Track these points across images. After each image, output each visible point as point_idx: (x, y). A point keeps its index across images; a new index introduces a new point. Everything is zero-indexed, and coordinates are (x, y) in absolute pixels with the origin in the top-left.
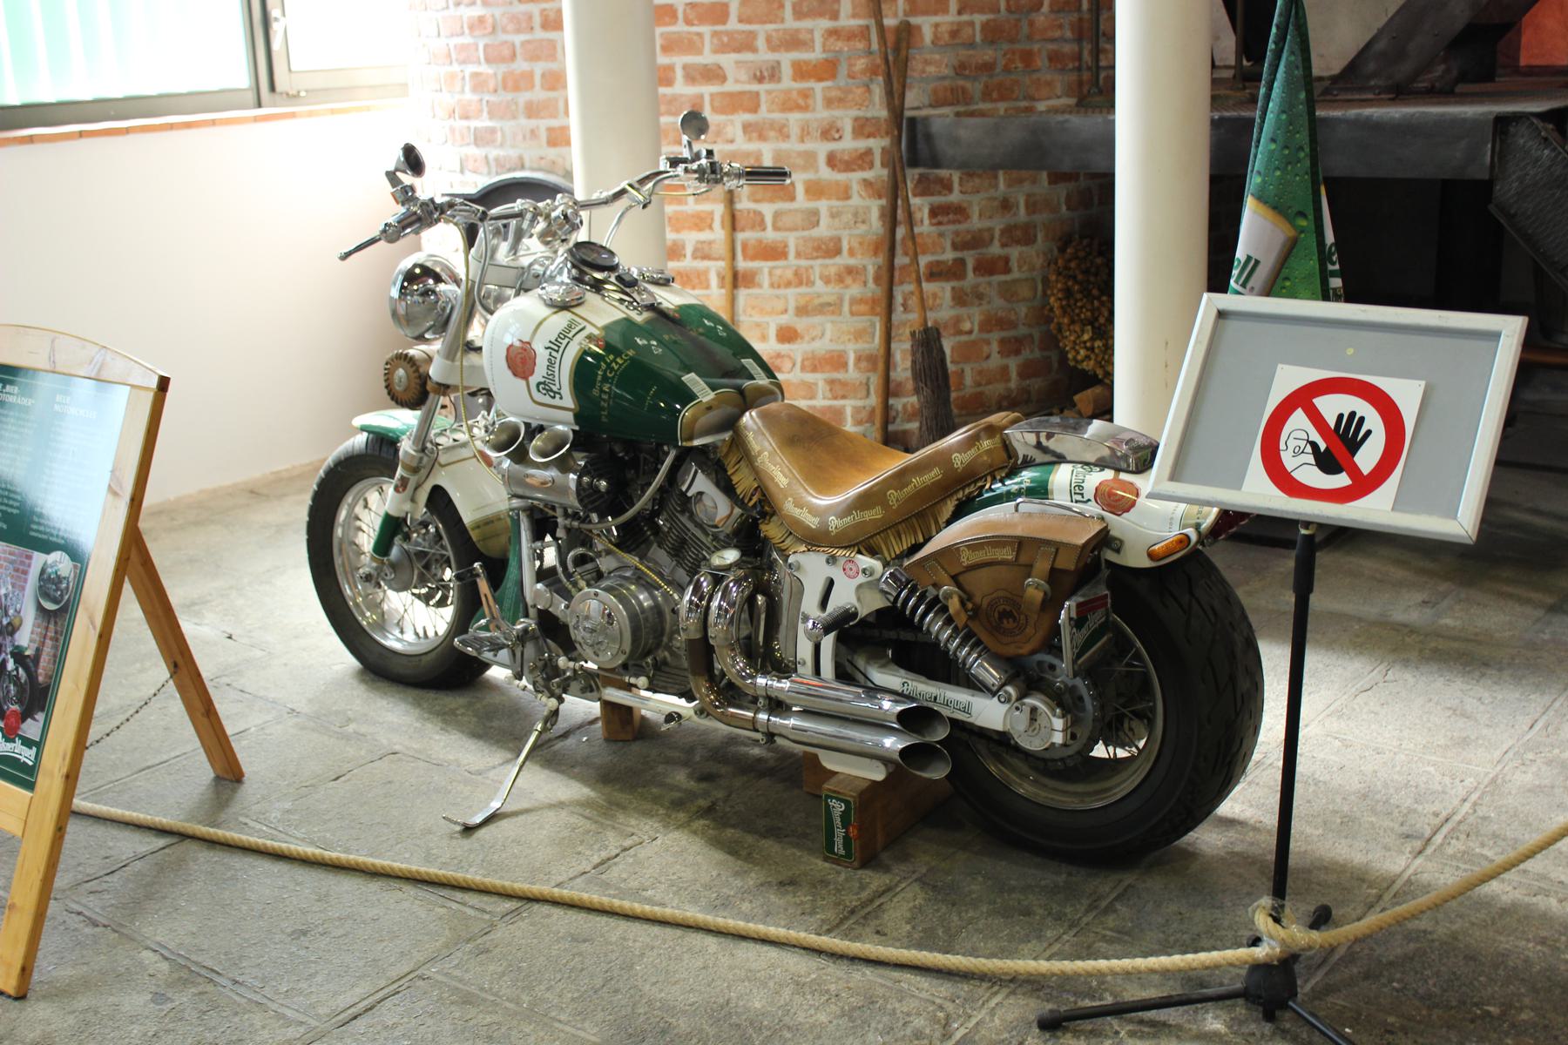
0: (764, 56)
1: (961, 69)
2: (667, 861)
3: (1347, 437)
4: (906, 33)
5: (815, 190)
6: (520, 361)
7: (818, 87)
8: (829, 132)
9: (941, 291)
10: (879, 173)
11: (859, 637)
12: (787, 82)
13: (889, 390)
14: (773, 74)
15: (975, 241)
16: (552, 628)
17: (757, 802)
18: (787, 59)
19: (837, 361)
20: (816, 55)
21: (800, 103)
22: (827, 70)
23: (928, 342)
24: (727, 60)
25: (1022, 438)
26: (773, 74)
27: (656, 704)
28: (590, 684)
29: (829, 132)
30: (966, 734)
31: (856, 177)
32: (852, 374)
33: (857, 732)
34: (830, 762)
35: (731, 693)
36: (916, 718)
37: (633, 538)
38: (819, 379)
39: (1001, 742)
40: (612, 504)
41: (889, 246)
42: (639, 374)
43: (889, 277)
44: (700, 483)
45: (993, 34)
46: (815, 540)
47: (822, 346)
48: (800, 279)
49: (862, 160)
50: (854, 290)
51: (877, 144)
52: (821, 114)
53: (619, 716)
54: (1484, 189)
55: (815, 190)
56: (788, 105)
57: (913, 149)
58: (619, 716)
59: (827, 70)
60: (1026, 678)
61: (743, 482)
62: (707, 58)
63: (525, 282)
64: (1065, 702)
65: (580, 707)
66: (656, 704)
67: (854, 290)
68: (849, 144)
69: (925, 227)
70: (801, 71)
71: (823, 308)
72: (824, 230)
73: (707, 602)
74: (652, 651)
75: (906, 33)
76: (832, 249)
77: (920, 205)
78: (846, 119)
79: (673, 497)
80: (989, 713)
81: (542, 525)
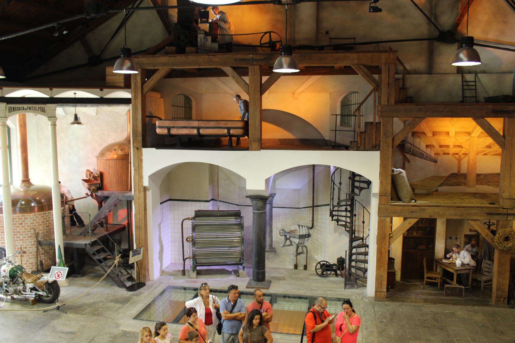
0: (24, 236)
1: (44, 235)
2: (17, 307)
3: (59, 275)
4: (38, 233)
5: (30, 247)
6: (4, 271)
7: (30, 238)
8: (31, 242)
9: (43, 255)
10: (36, 245)
11: (32, 289)
12: (27, 238)
13: (38, 265)
14: (25, 237)
15: (46, 251)
16: (7, 291)
17: (25, 302)
18: (26, 236)
19: (32, 263)
20: (29, 235)
21: (28, 240)
22: (30, 237)
23: (41, 262)
24: (20, 236)
25: (43, 274)
26: (25, 237)
27: (15, 296)
28: (10, 295)
29: (31, 242)
30: (39, 295)
31: (33, 246)
32: (34, 264)
33: (31, 296)
34: (30, 298)
35: (22, 294)
36: (36, 294)
37: (13, 283)
38: (31, 265)
39: (42, 295)
40: (12, 281)
41: (37, 252)
42: (15, 271)
43: (37, 255)
44: (19, 279)
45: (47, 232)
46: (28, 283)
47: (31, 262)
48: (28, 256)
49: (34, 244)
50: (34, 256)
51: (36, 243)
52: (30, 241)
53: (12, 298)
54: (85, 249)
55: (30, 247)
56: (27, 240)
57: (39, 243)
58: (12, 298)
59: (30, 237)
60: (43, 290)
61: (23, 279)
62: (18, 236)
63: (4, 264)
64: (46, 292)
65: (9, 297)
66: (15, 296)
67: (34, 256)
68: (33, 243)
69: (41, 250)
70: (28, 237)
71: (31, 258)
72: (31, 251)
73: (20, 288)
74: (16, 292)
75: (38, 233)
76: (32, 253)
77: (40, 248)
78: (32, 241)
79: (17, 280)
80: (41, 293)
81: (6, 283)
